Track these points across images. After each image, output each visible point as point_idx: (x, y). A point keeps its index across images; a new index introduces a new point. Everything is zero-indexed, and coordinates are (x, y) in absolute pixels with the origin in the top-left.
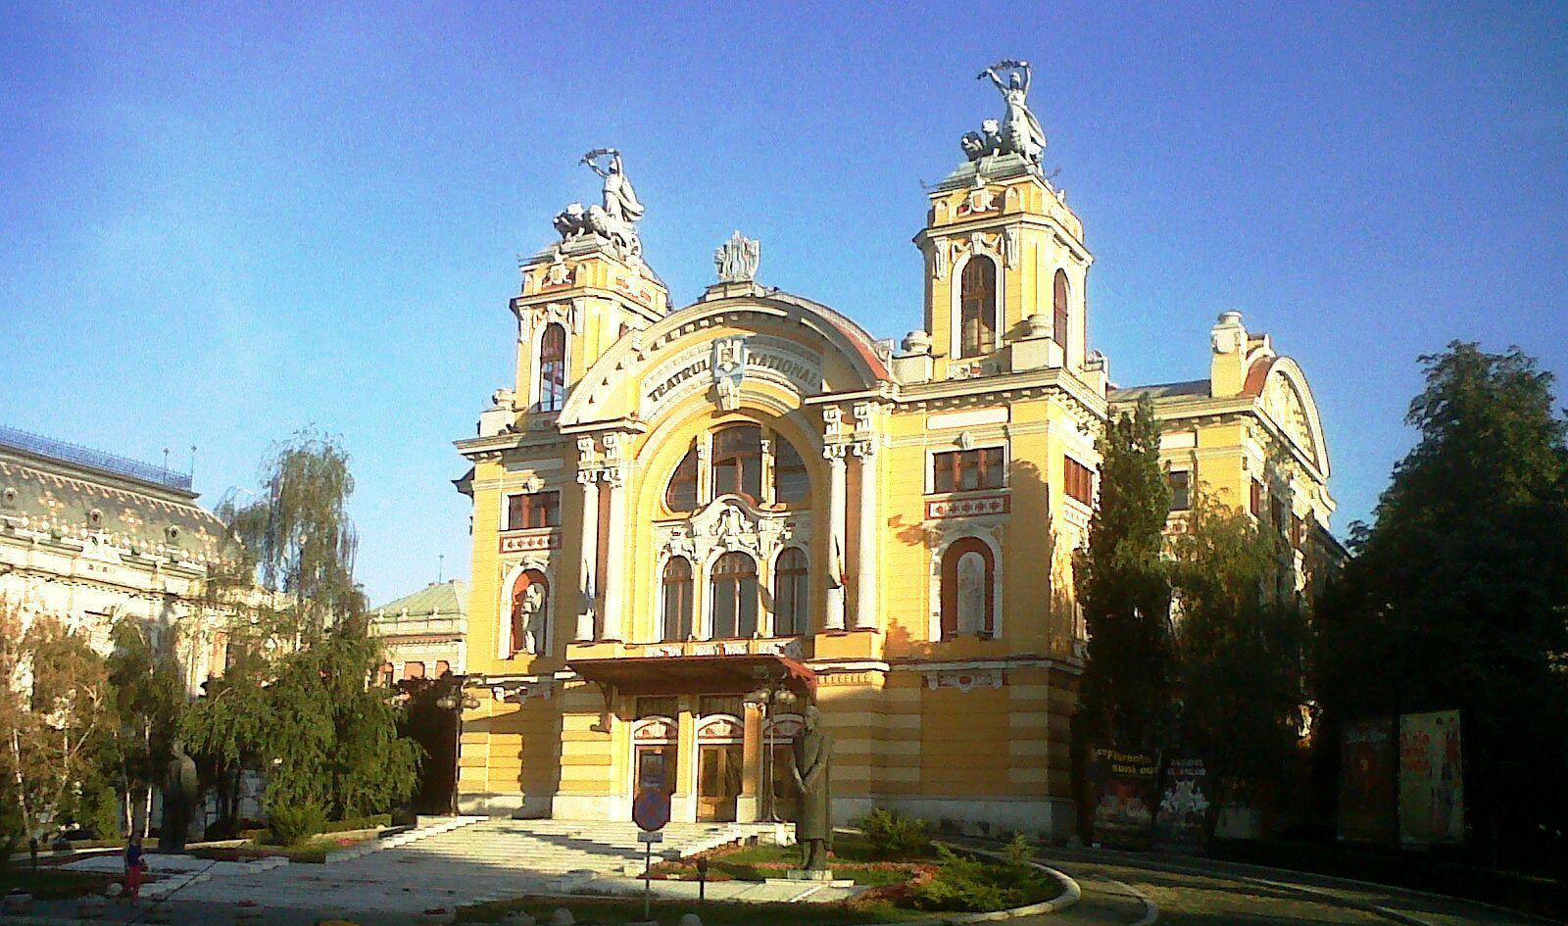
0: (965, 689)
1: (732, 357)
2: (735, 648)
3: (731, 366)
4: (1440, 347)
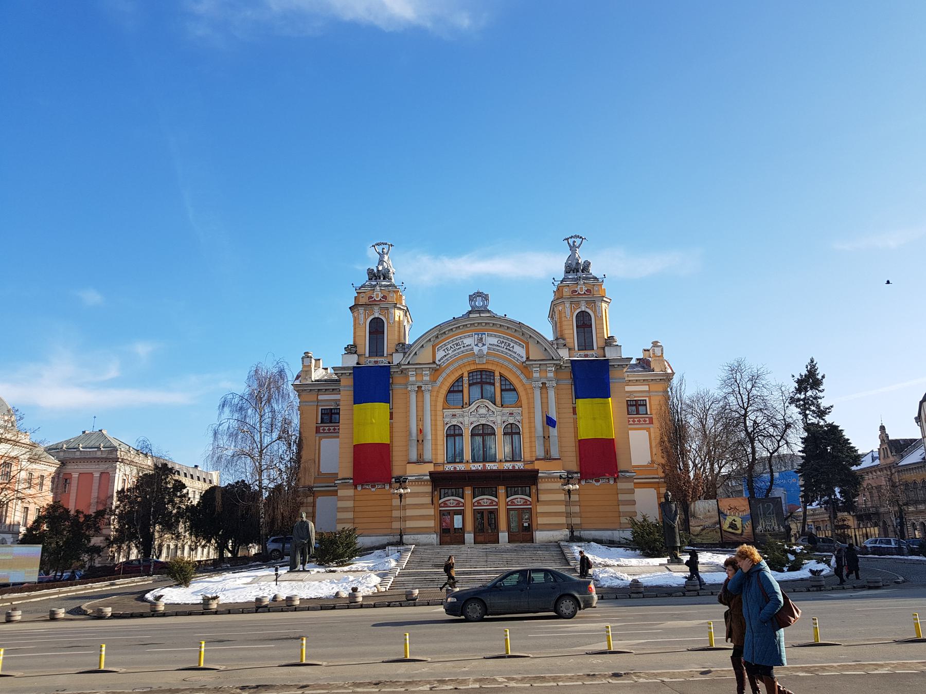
0: (599, 484)
1: (482, 341)
2: (491, 466)
3: (482, 345)
4: (732, 360)
